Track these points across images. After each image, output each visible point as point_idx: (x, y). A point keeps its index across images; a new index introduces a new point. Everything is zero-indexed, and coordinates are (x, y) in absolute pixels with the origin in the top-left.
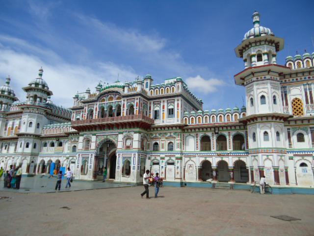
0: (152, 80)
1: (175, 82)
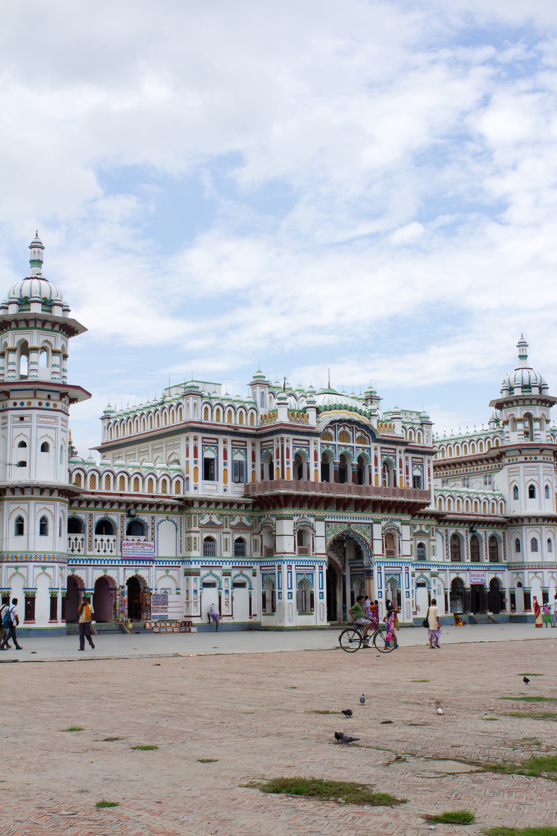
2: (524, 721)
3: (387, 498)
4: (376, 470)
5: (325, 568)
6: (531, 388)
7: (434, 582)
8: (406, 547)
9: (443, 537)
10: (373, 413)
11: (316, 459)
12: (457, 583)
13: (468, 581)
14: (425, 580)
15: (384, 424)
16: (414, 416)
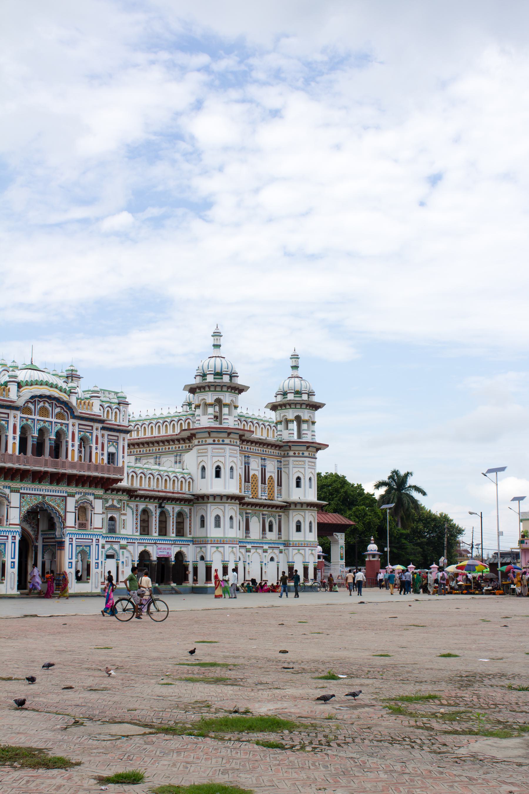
2: (198, 685)
3: (82, 473)
4: (73, 446)
5: (18, 538)
6: (222, 376)
7: (123, 554)
8: (98, 520)
9: (133, 512)
10: (72, 391)
12: (144, 555)
13: (155, 554)
14: (114, 552)
15: (83, 401)
16: (112, 396)
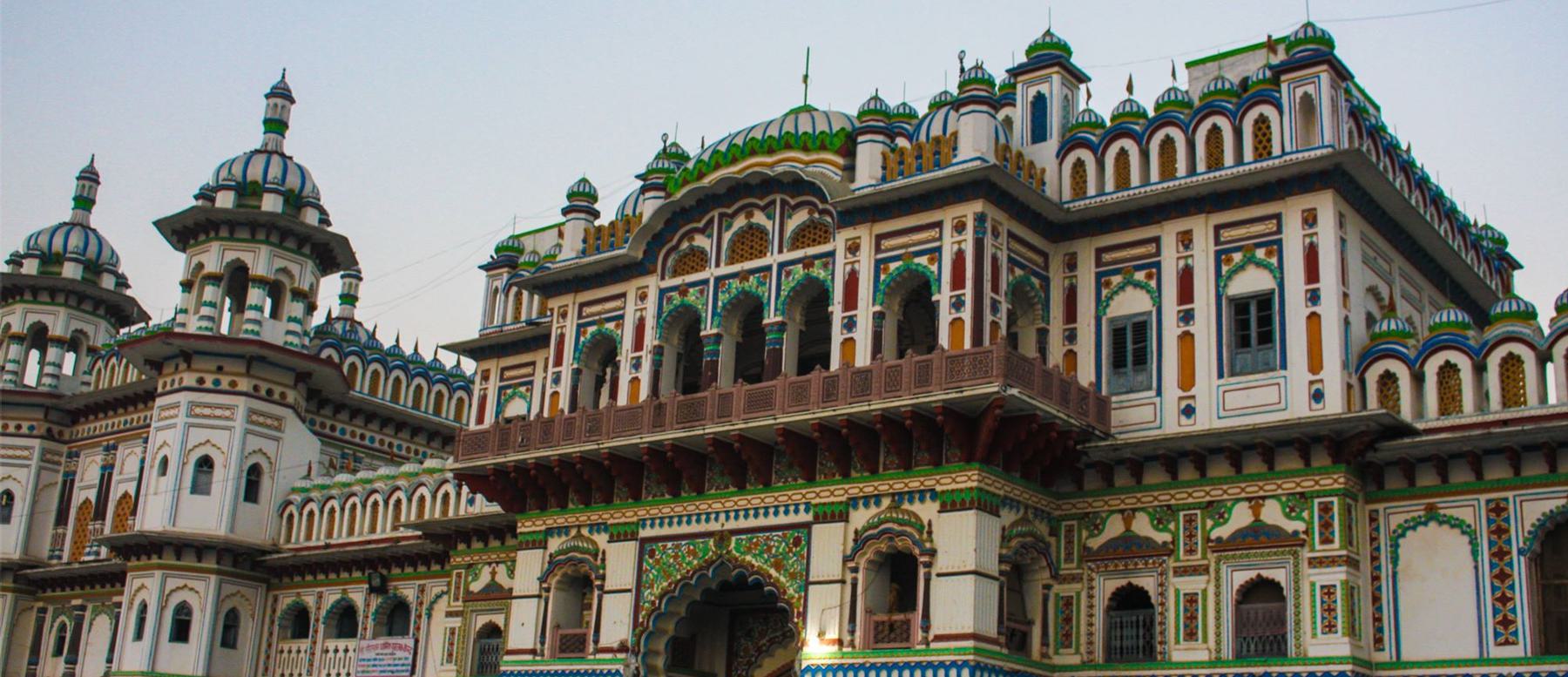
0: (1081, 78)
1: (1278, 72)
4: (850, 324)
9: (1473, 542)
11: (638, 344)
